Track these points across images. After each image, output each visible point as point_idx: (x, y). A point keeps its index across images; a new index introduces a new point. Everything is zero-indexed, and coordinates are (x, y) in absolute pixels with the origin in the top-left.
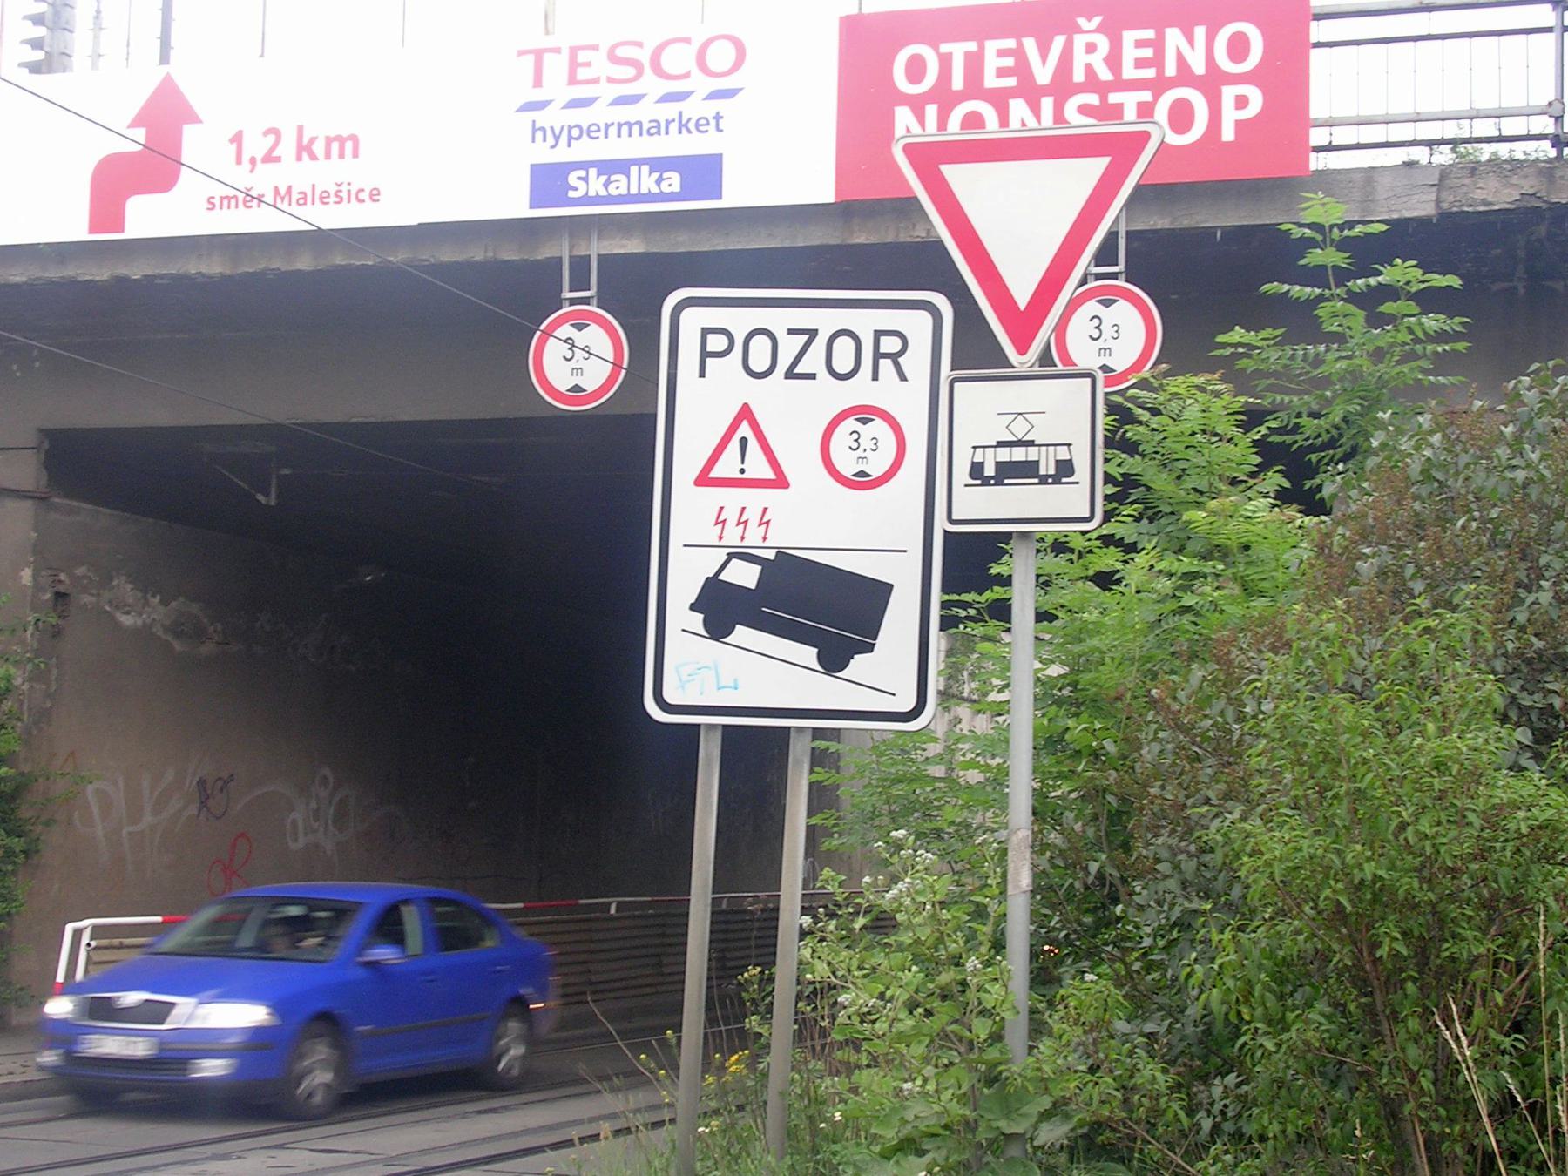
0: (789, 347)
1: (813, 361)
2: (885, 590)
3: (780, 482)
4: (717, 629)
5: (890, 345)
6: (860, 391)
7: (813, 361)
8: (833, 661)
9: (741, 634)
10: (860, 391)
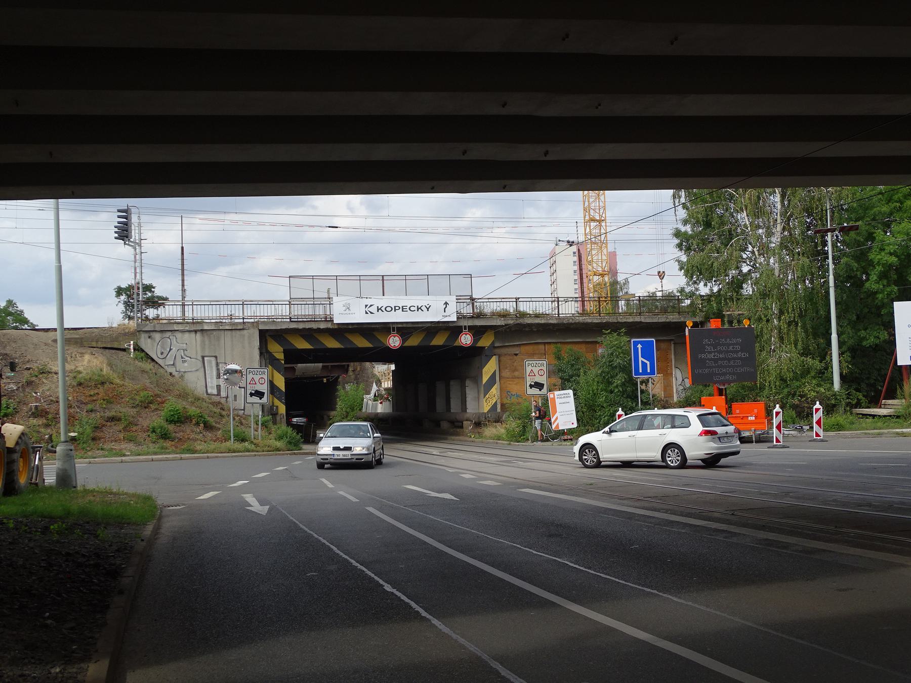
1: (258, 374)
2: (264, 393)
3: (256, 384)
4: (251, 396)
6: (261, 376)
8: (261, 399)
10: (261, 376)
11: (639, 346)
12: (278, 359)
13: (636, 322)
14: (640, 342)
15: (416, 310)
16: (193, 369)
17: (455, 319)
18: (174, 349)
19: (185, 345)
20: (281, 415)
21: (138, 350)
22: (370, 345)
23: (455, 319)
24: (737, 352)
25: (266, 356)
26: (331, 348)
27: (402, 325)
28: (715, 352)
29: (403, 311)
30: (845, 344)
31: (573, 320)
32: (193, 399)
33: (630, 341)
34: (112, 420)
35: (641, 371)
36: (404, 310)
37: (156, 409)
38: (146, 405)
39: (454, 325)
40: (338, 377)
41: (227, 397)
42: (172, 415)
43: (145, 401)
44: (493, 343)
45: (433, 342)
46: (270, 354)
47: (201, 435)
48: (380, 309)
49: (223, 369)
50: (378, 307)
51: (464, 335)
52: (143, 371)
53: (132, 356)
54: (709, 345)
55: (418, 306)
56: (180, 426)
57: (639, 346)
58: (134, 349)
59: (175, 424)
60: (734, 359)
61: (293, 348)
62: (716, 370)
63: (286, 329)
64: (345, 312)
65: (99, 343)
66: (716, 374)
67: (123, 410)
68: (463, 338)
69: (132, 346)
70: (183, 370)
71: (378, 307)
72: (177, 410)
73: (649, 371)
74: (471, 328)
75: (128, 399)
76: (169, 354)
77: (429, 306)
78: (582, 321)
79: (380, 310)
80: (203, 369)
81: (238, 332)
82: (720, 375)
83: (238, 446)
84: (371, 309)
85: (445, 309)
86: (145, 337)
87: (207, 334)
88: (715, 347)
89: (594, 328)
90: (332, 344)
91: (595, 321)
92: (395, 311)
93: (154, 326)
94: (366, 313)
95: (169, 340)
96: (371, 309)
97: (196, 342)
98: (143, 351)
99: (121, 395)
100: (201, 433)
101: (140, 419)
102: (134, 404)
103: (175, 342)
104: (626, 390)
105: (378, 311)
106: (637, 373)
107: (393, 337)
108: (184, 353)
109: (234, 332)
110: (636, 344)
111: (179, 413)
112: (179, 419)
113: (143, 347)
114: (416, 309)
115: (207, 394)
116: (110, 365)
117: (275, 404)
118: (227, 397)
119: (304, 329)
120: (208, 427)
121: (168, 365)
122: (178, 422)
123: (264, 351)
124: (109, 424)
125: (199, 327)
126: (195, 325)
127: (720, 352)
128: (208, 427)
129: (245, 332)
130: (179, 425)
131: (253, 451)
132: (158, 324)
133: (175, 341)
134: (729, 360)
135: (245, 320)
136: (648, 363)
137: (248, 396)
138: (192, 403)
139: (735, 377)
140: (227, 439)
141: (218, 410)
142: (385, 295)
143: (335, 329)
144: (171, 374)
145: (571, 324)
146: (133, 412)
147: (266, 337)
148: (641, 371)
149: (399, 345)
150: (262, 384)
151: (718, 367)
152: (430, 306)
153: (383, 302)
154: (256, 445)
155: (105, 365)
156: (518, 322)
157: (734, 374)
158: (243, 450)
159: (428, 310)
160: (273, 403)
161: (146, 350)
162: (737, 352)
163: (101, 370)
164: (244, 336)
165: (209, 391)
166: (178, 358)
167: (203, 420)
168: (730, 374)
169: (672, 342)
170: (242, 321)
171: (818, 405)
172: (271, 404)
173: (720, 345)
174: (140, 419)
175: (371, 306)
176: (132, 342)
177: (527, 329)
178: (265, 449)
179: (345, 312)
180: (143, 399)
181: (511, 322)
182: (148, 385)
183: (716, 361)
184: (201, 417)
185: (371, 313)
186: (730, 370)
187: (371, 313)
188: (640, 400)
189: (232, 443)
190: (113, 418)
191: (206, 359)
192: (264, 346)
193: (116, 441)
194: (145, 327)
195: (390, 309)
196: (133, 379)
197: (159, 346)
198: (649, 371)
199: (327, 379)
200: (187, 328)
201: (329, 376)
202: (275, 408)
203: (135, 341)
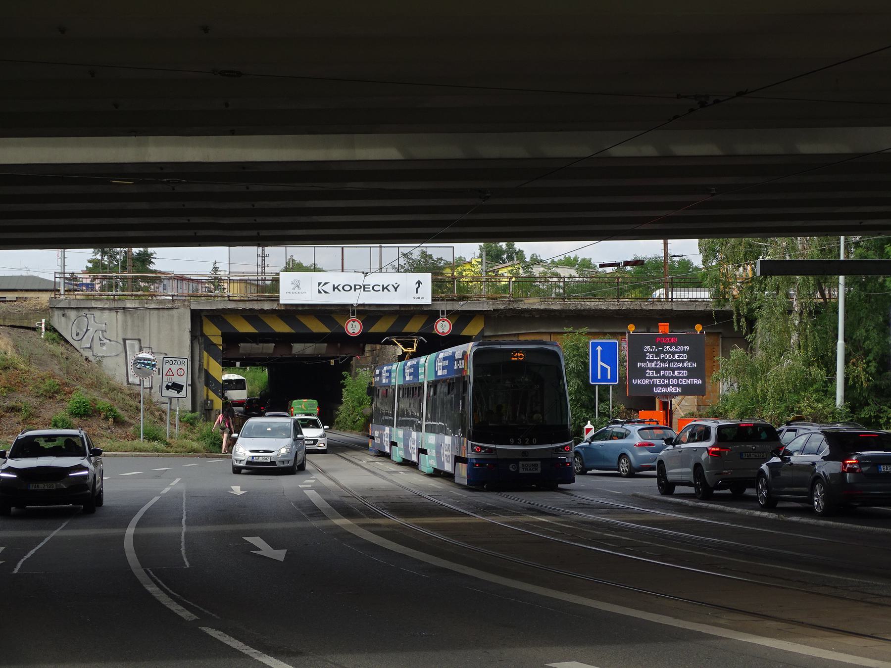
0: (174, 362)
1: (176, 364)
2: (182, 386)
4: (168, 389)
5: (183, 362)
6: (181, 367)
7: (176, 364)
8: (178, 392)
9: (170, 390)
10: (181, 367)
11: (599, 348)
12: (215, 345)
13: (666, 310)
14: (601, 344)
15: (381, 290)
16: (114, 354)
17: (428, 301)
18: (91, 329)
19: (104, 325)
20: (216, 410)
21: (50, 330)
22: (327, 330)
23: (428, 301)
24: (683, 361)
25: (202, 340)
26: (279, 333)
27: (364, 307)
28: (657, 361)
29: (364, 291)
30: (871, 353)
31: (582, 305)
32: (107, 390)
33: (588, 343)
34: (11, 410)
35: (599, 377)
36: (366, 289)
37: (62, 400)
38: (51, 395)
39: (429, 309)
40: (351, 359)
41: (151, 388)
42: (78, 408)
43: (50, 391)
44: (483, 330)
45: (405, 328)
46: (206, 338)
47: (109, 431)
48: (337, 288)
49: (135, 355)
50: (334, 285)
51: (441, 322)
52: (54, 355)
53: (42, 337)
54: (650, 353)
55: (383, 286)
56: (86, 420)
57: (599, 348)
58: (46, 329)
59: (81, 417)
60: (679, 369)
61: (232, 331)
62: (657, 381)
63: (223, 310)
64: (293, 291)
65: (7, 320)
66: (657, 386)
67: (22, 399)
68: (439, 325)
69: (43, 325)
70: (102, 355)
71: (334, 285)
72: (84, 402)
73: (609, 377)
74: (450, 314)
75: (31, 388)
76: (85, 337)
77: (397, 285)
78: (593, 308)
79: (336, 290)
80: (124, 354)
81: (166, 312)
82: (662, 386)
83: (147, 445)
84: (325, 288)
85: (417, 289)
86: (58, 315)
87: (130, 313)
88: (657, 354)
89: (615, 316)
90: (281, 327)
91: (612, 308)
92: (355, 291)
93: (70, 303)
94: (320, 292)
95: (86, 319)
96: (325, 288)
97: (117, 322)
98: (55, 331)
99: (25, 382)
100: (109, 428)
101: (43, 411)
102: (38, 393)
103: (93, 322)
104: (580, 399)
105: (334, 290)
106: (595, 378)
107: (352, 322)
108: (103, 335)
109: (161, 310)
110: (595, 345)
111: (86, 405)
112: (85, 413)
113: (56, 326)
114: (381, 287)
115: (128, 383)
116: (16, 347)
117: (210, 398)
118: (151, 388)
119: (244, 310)
120: (118, 422)
121: (84, 348)
122: (84, 415)
123: (198, 333)
124: (8, 414)
125: (121, 305)
126: (116, 303)
127: (663, 361)
128: (118, 422)
129: (175, 311)
130: (85, 419)
131: (162, 451)
132: (73, 299)
133: (92, 320)
134: (673, 370)
135: (175, 298)
136: (609, 368)
137: (164, 388)
138: (106, 394)
139: (679, 390)
140: (136, 437)
141: (134, 403)
142: (345, 270)
143: (283, 310)
144: (87, 359)
145: (580, 310)
146: (36, 402)
147: (201, 317)
148: (599, 377)
149: (359, 332)
150: (181, 376)
151: (660, 377)
152: (399, 285)
153: (340, 279)
154: (168, 444)
155: (10, 348)
156: (511, 307)
157: (678, 385)
158: (151, 449)
159: (396, 291)
160: (207, 396)
161: (60, 331)
162: (683, 361)
163: (5, 353)
164: (173, 316)
165: (131, 380)
166: (96, 340)
167: (112, 414)
168: (673, 386)
169: (720, 336)
170: (171, 298)
171: (589, 425)
172: (205, 397)
173: (664, 353)
174: (43, 411)
175: (326, 284)
176: (43, 321)
177: (527, 315)
178: (178, 450)
179: (293, 291)
180: (48, 388)
181: (502, 307)
182: (57, 371)
183: (658, 371)
184: (111, 410)
185: (326, 292)
186: (674, 381)
187: (326, 292)
188: (597, 411)
189: (142, 441)
190: (13, 408)
191: (127, 342)
192: (199, 328)
193: (13, 434)
194: (58, 303)
195: (348, 288)
196: (40, 365)
197: (74, 326)
198: (609, 377)
199: (334, 361)
200: (107, 306)
201: (338, 357)
202: (209, 402)
203: (48, 320)
